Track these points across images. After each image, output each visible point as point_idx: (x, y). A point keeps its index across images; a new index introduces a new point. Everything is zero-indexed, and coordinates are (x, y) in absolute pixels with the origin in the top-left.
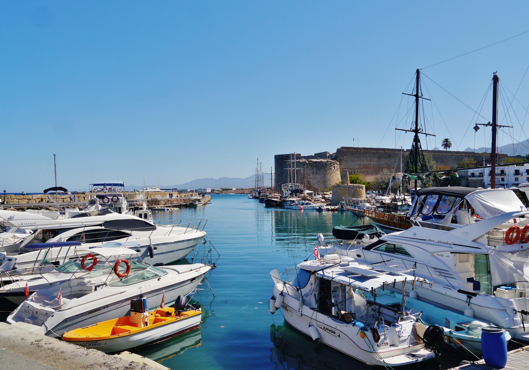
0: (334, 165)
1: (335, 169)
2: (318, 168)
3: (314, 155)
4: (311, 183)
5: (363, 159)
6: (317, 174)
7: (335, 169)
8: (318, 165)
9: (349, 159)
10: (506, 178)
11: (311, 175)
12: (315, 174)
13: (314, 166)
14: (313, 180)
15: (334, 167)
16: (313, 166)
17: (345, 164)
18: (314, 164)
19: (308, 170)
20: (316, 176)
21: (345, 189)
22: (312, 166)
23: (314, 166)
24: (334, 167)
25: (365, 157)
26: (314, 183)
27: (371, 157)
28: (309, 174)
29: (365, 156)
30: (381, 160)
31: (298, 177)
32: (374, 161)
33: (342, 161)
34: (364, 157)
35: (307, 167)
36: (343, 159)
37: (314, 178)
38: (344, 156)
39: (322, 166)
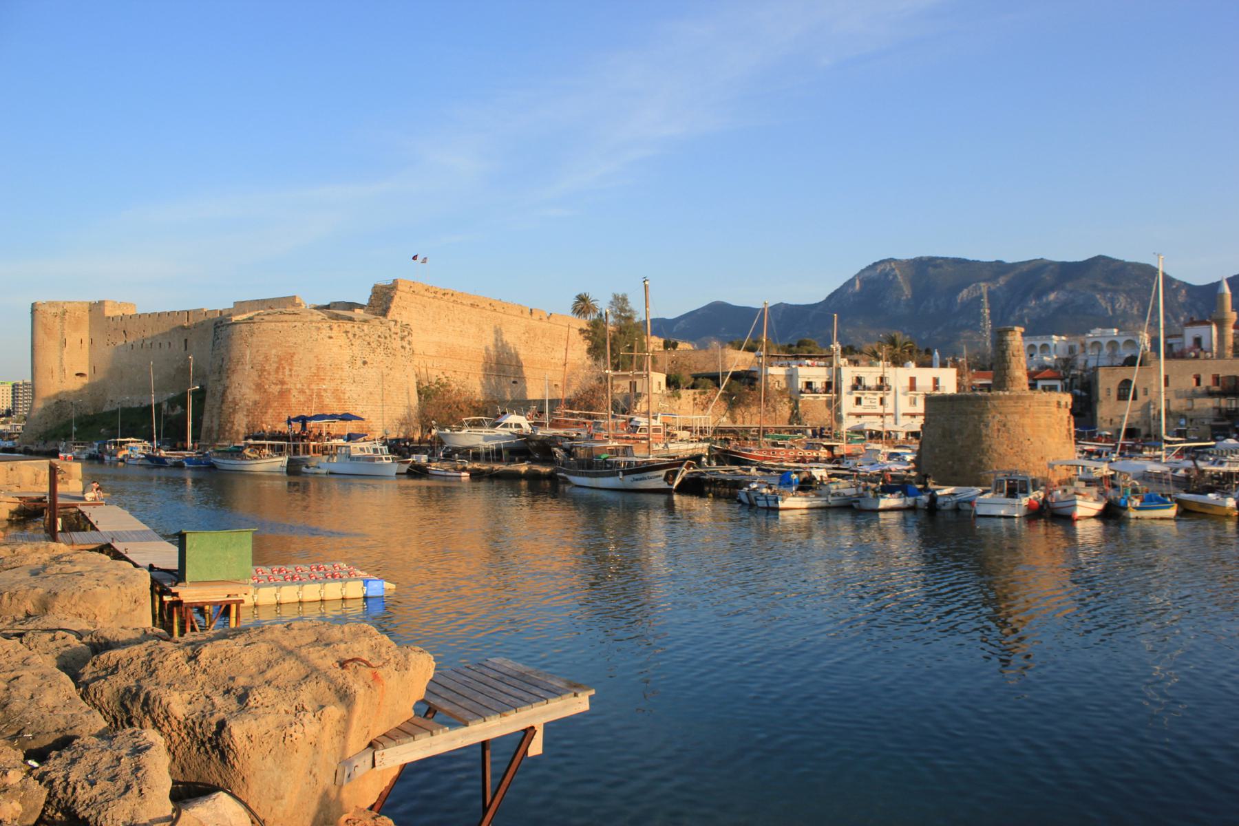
2: (369, 344)
3: (232, 306)
5: (447, 327)
6: (365, 363)
8: (366, 331)
10: (889, 399)
12: (359, 363)
13: (355, 335)
14: (353, 387)
16: (350, 335)
18: (356, 329)
21: (1046, 413)
22: (347, 332)
23: (355, 335)
26: (355, 396)
30: (483, 335)
31: (293, 373)
35: (330, 338)
38: (403, 312)
39: (379, 336)
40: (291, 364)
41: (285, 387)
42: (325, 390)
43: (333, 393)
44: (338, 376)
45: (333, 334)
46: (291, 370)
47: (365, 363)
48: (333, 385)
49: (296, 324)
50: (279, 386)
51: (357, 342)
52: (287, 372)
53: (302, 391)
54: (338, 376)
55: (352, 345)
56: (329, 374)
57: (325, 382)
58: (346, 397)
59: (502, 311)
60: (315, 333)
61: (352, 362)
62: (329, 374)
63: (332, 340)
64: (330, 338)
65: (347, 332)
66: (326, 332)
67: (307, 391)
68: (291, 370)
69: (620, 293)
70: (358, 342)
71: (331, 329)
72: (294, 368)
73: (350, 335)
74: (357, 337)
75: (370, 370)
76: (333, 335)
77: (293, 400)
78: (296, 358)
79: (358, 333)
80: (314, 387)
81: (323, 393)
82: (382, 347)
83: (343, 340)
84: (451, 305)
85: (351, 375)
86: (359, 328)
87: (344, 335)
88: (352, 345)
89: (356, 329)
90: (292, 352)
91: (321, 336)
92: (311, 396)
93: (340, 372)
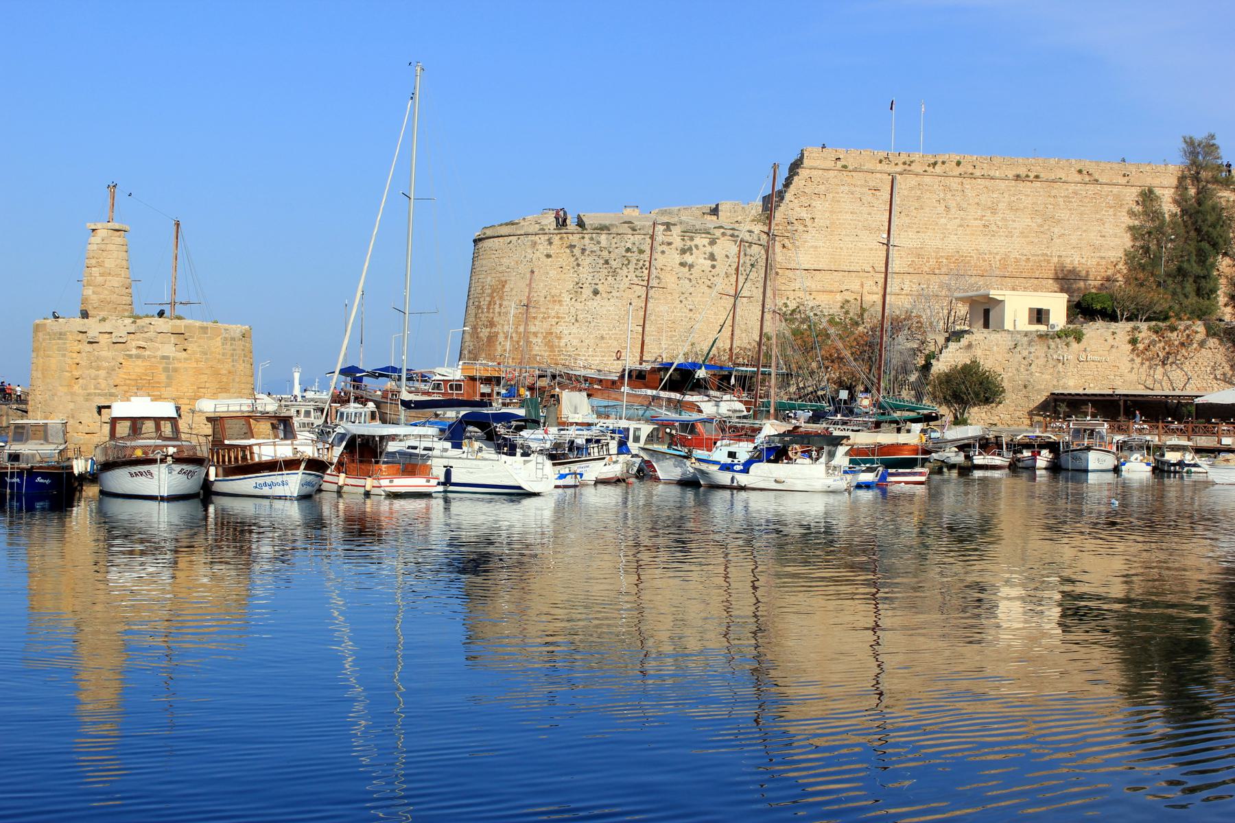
0: (713, 242)
1: (713, 267)
2: (607, 262)
4: (562, 344)
5: (943, 221)
6: (596, 293)
7: (713, 267)
8: (604, 243)
9: (849, 216)
11: (566, 298)
12: (587, 292)
13: (583, 250)
14: (574, 330)
15: (712, 257)
16: (577, 251)
17: (821, 244)
18: (587, 241)
19: (553, 273)
20: (594, 304)
22: (572, 247)
23: (583, 250)
25: (953, 211)
26: (575, 342)
27: (994, 213)
28: (554, 291)
29: (952, 204)
32: (1010, 235)
33: (801, 228)
35: (548, 256)
36: (804, 214)
37: (580, 317)
38: (817, 203)
39: (628, 250)
40: (501, 298)
41: (493, 330)
42: (535, 334)
43: (545, 338)
44: (553, 313)
46: (501, 305)
47: (596, 293)
48: (546, 325)
49: (511, 238)
50: (488, 330)
51: (586, 261)
52: (497, 310)
54: (553, 313)
55: (578, 265)
56: (543, 310)
57: (537, 323)
58: (562, 344)
59: (1124, 181)
60: (530, 251)
62: (543, 310)
63: (550, 259)
64: (548, 256)
65: (572, 247)
66: (543, 248)
68: (501, 305)
69: (1199, 136)
70: (589, 260)
71: (550, 243)
72: (505, 303)
73: (577, 251)
74: (587, 252)
75: (605, 302)
78: (507, 288)
79: (590, 246)
82: (632, 267)
83: (565, 258)
84: (954, 183)
86: (592, 239)
87: (568, 251)
88: (578, 265)
89: (587, 241)
90: (503, 279)
91: (538, 254)
92: (518, 342)
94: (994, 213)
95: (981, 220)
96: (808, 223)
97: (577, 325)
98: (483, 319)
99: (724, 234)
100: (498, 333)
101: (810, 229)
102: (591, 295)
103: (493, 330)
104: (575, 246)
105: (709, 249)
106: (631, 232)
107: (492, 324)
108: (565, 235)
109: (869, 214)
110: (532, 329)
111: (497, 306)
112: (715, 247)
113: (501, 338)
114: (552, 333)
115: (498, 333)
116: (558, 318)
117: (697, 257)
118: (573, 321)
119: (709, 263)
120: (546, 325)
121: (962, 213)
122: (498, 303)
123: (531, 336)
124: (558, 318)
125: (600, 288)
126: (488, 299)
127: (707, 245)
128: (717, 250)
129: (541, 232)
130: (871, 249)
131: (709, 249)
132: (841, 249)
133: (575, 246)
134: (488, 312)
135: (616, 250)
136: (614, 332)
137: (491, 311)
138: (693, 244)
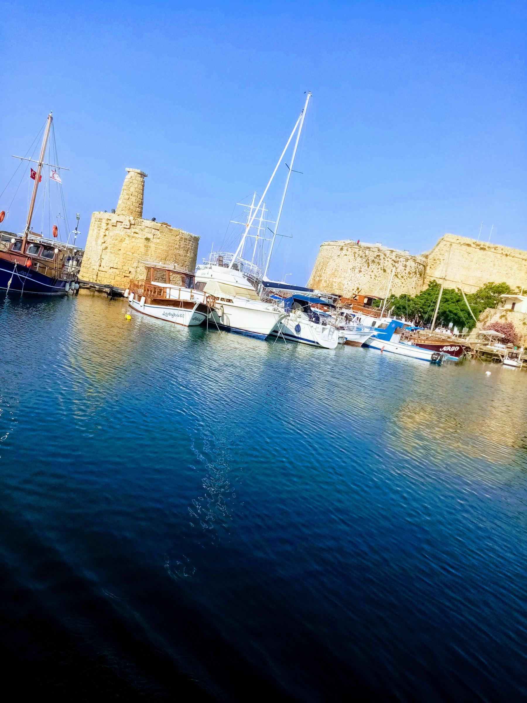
0: (407, 260)
6: (360, 271)
12: (357, 271)
15: (405, 266)
18: (361, 252)
20: (358, 275)
24: (405, 266)
33: (438, 262)
34: (494, 265)
37: (353, 279)
40: (326, 267)
42: (335, 282)
44: (343, 276)
45: (348, 253)
47: (360, 271)
48: (340, 280)
49: (334, 246)
50: (319, 278)
53: (326, 282)
54: (343, 276)
61: (354, 268)
62: (339, 274)
67: (328, 281)
72: (327, 269)
76: (347, 254)
77: (321, 285)
80: (331, 280)
81: (334, 284)
84: (499, 256)
85: (350, 276)
86: (363, 251)
92: (328, 284)
93: (345, 273)
94: (511, 269)
95: (506, 271)
96: (442, 261)
97: (351, 281)
98: (318, 274)
99: (411, 258)
100: (322, 280)
101: (442, 263)
102: (358, 272)
103: (321, 278)
104: (356, 253)
105: (405, 263)
106: (378, 251)
107: (320, 276)
108: (353, 248)
109: (465, 262)
110: (334, 280)
111: (324, 270)
112: (407, 262)
113: (323, 281)
114: (341, 283)
115: (322, 280)
116: (345, 278)
117: (400, 265)
118: (350, 280)
119: (404, 268)
120: (340, 280)
121: (499, 267)
122: (324, 269)
123: (334, 282)
124: (345, 278)
125: (362, 270)
126: (321, 267)
127: (404, 261)
128: (407, 263)
129: (345, 246)
130: (463, 275)
131: (405, 263)
132: (452, 272)
133: (356, 253)
134: (320, 271)
135: (371, 257)
136: (363, 286)
137: (321, 271)
138: (399, 260)
